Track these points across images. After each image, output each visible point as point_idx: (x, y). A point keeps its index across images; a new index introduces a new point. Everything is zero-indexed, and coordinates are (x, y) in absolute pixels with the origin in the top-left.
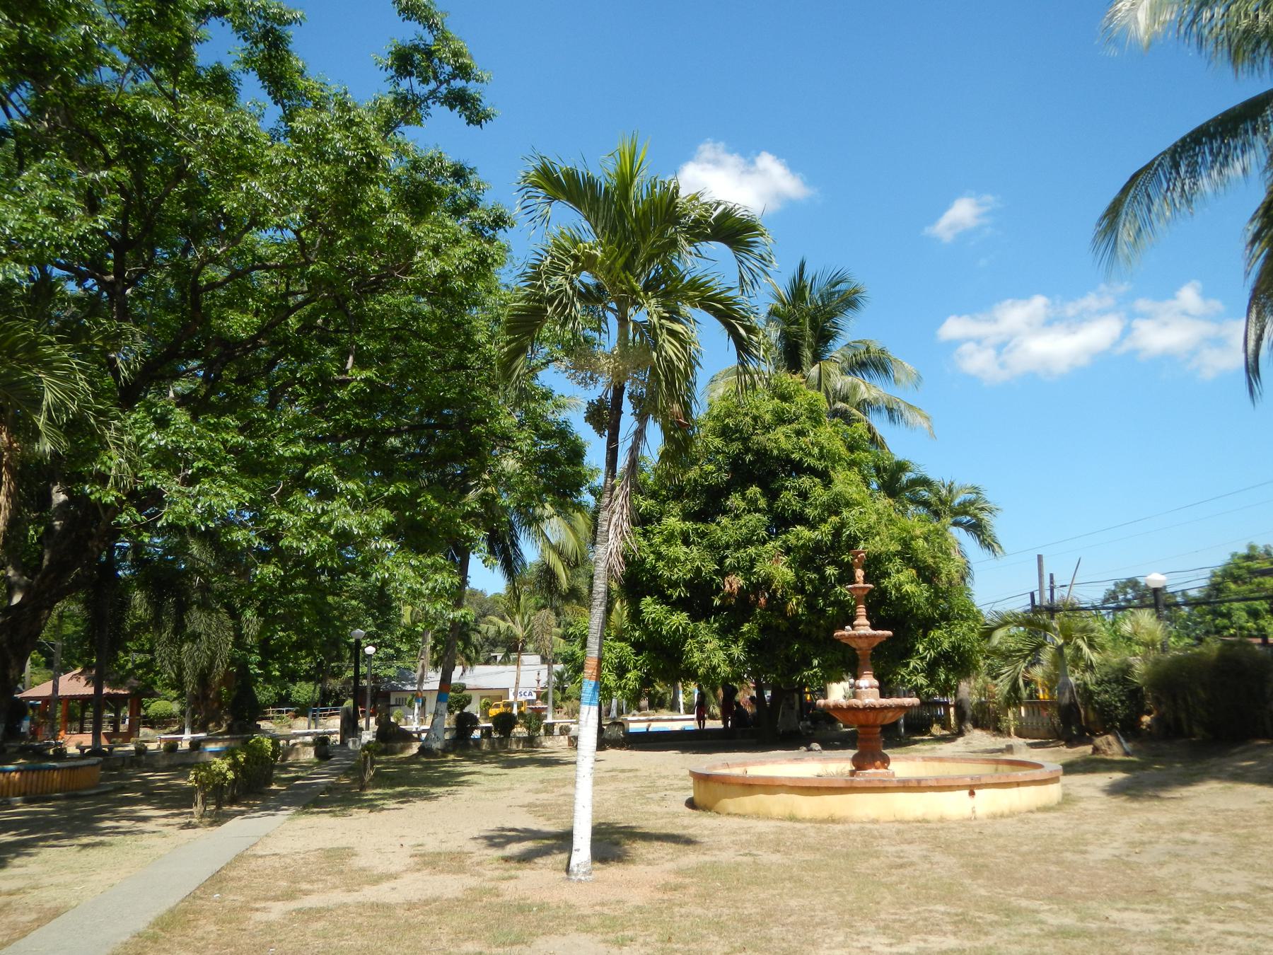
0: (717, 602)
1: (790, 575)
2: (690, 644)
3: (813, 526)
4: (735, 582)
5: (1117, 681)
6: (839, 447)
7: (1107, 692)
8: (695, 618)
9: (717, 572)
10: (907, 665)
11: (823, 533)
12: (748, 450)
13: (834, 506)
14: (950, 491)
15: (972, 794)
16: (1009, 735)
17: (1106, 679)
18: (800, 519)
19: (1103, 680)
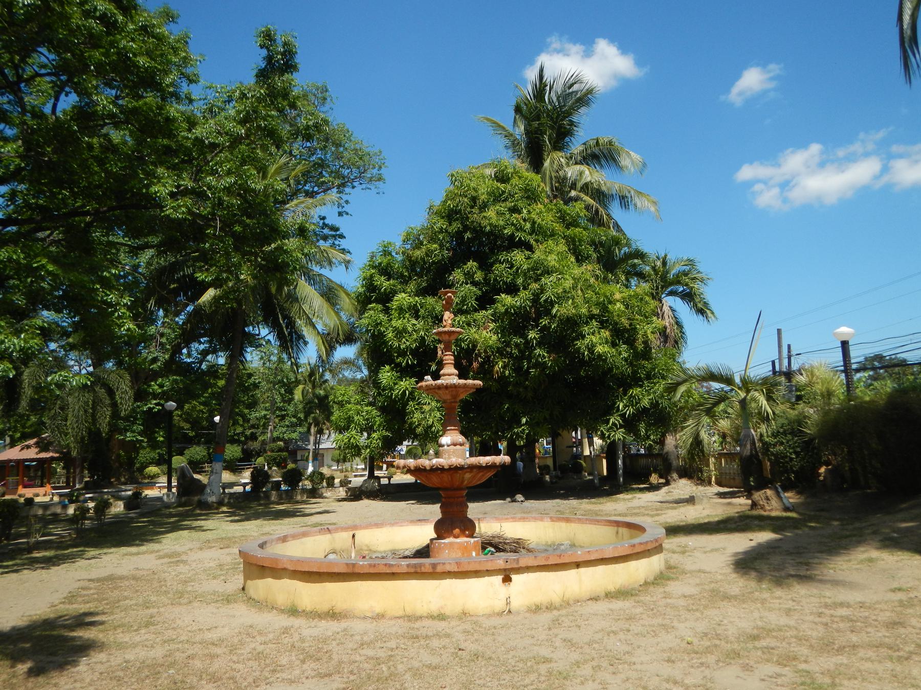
5: (793, 433)
7: (782, 443)
10: (607, 422)
11: (521, 300)
12: (466, 228)
14: (664, 263)
15: (507, 579)
16: (710, 483)
17: (781, 430)
19: (778, 432)
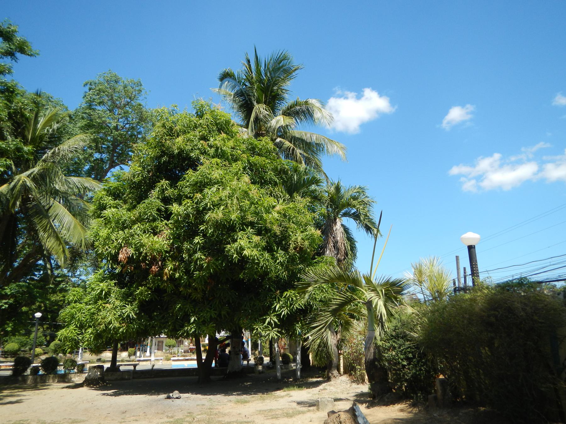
17: (394, 334)
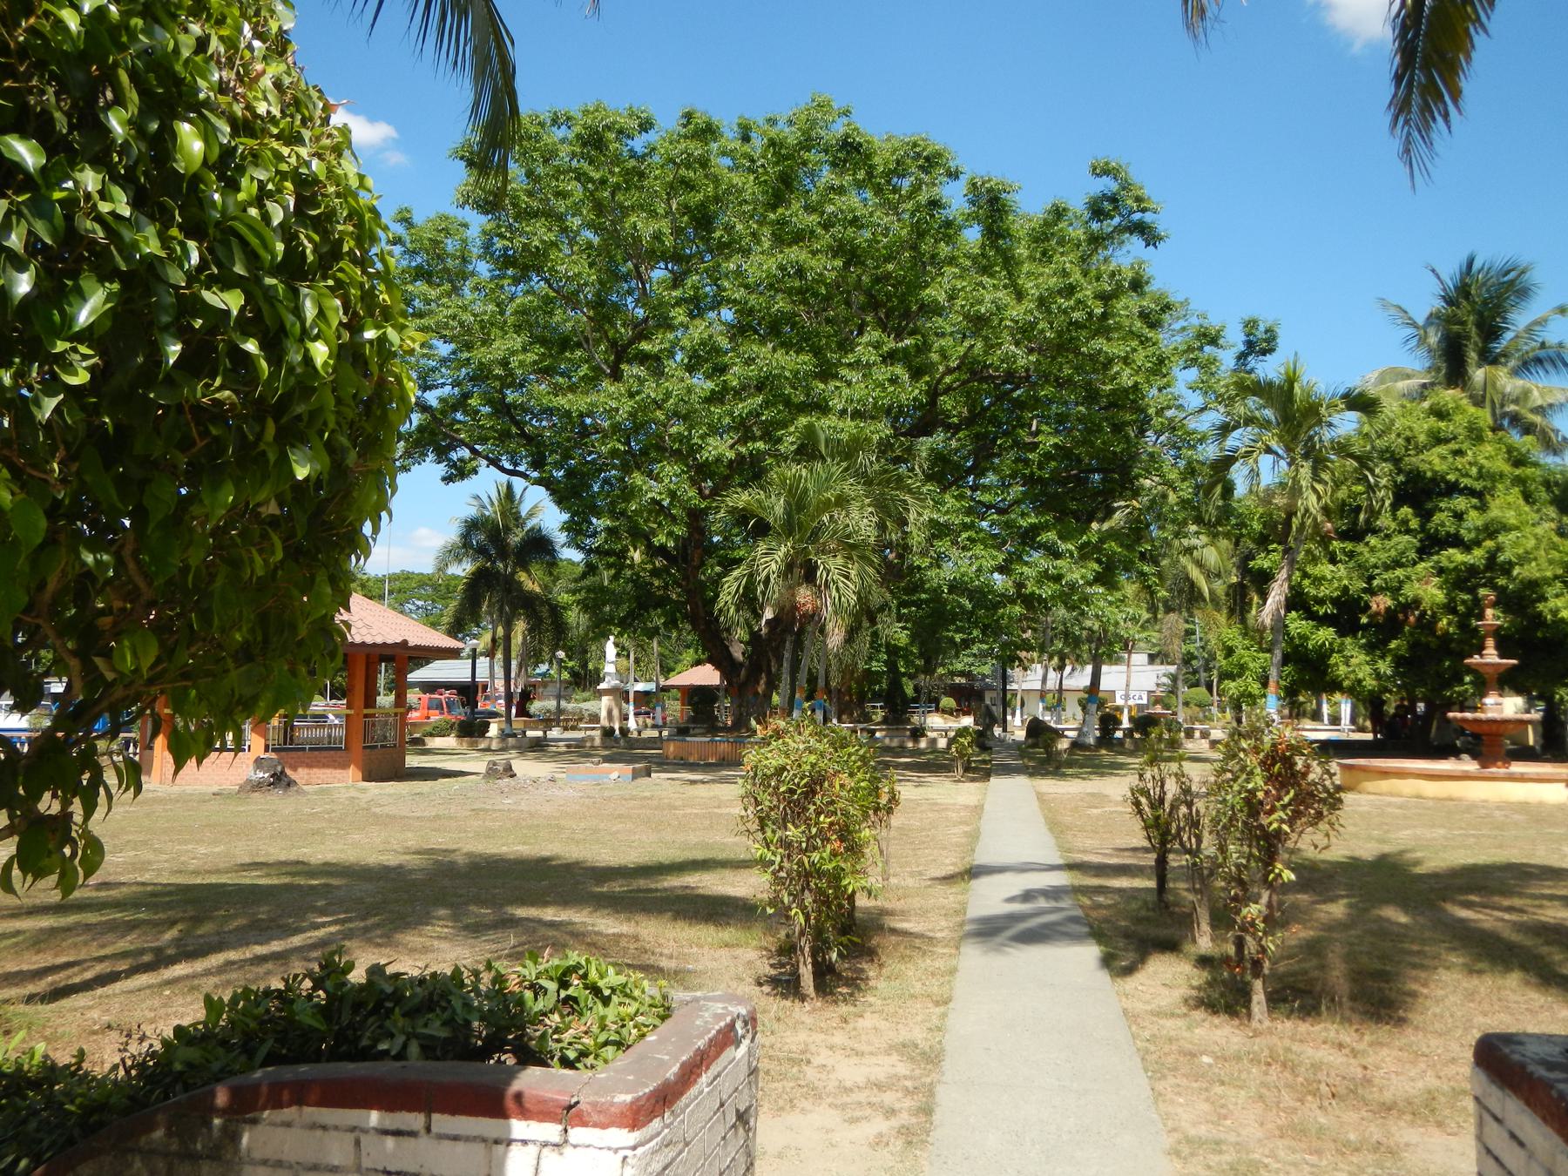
0: (1364, 620)
1: (1440, 596)
2: (1335, 659)
3: (1467, 547)
4: (1381, 603)
6: (1501, 465)
8: (1342, 633)
9: (1365, 591)
11: (1477, 556)
13: (1492, 530)
18: (1455, 541)
